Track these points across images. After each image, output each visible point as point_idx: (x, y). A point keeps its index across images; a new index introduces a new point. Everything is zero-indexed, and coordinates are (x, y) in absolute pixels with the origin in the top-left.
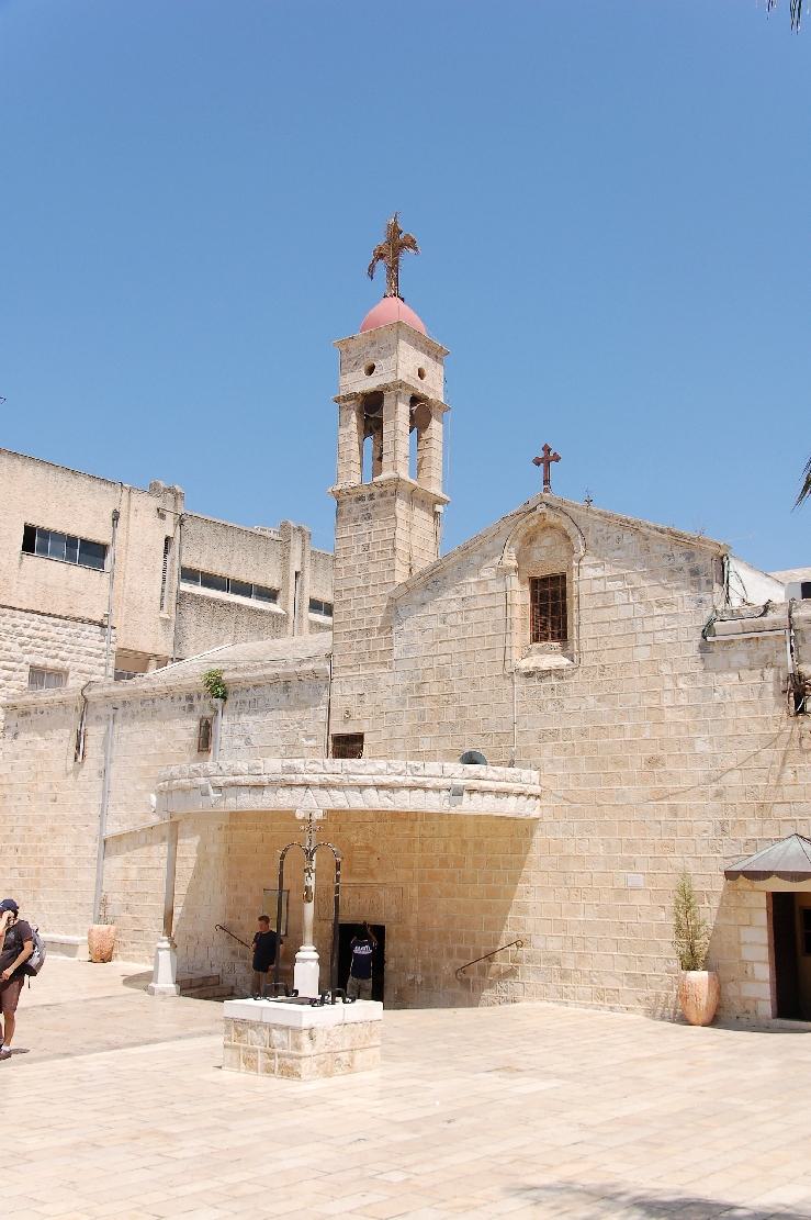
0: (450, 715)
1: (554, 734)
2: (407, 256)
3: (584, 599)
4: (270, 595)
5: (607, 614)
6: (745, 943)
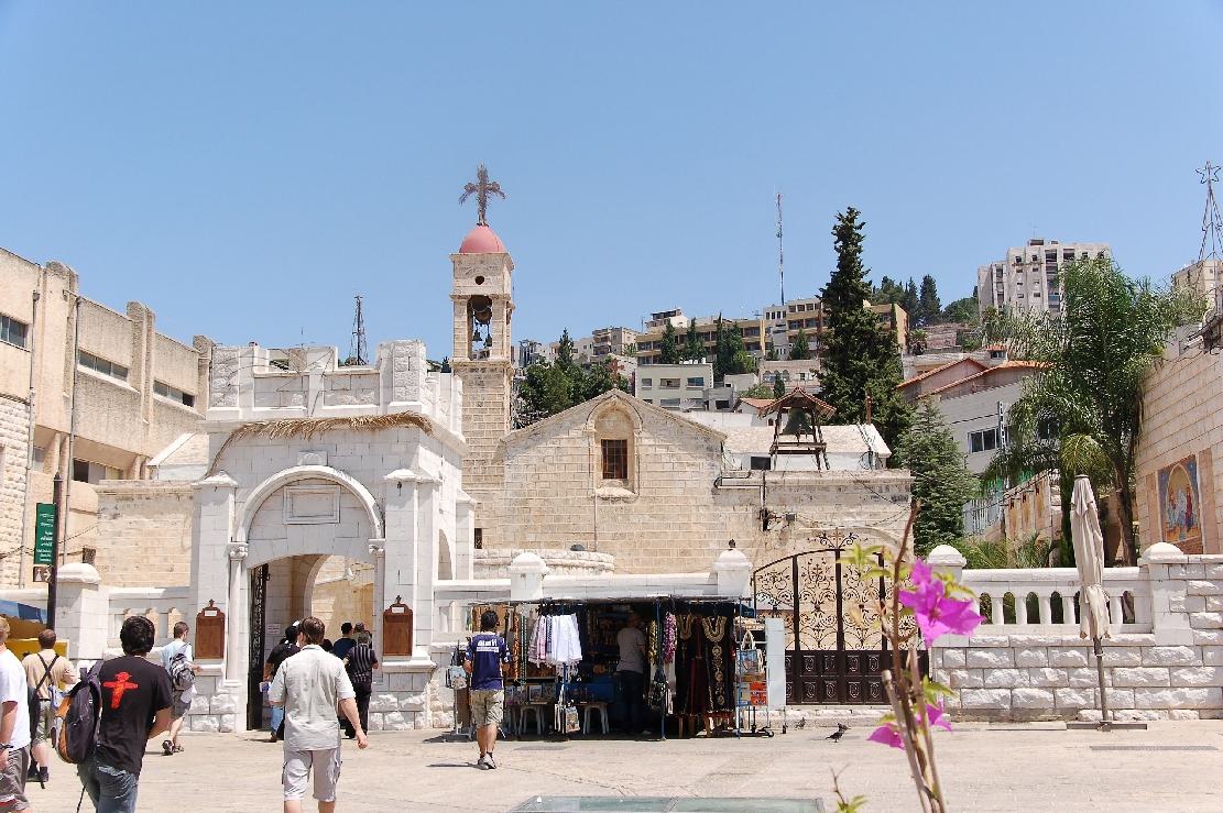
1: (623, 536)
2: (493, 200)
4: (122, 372)
5: (658, 467)
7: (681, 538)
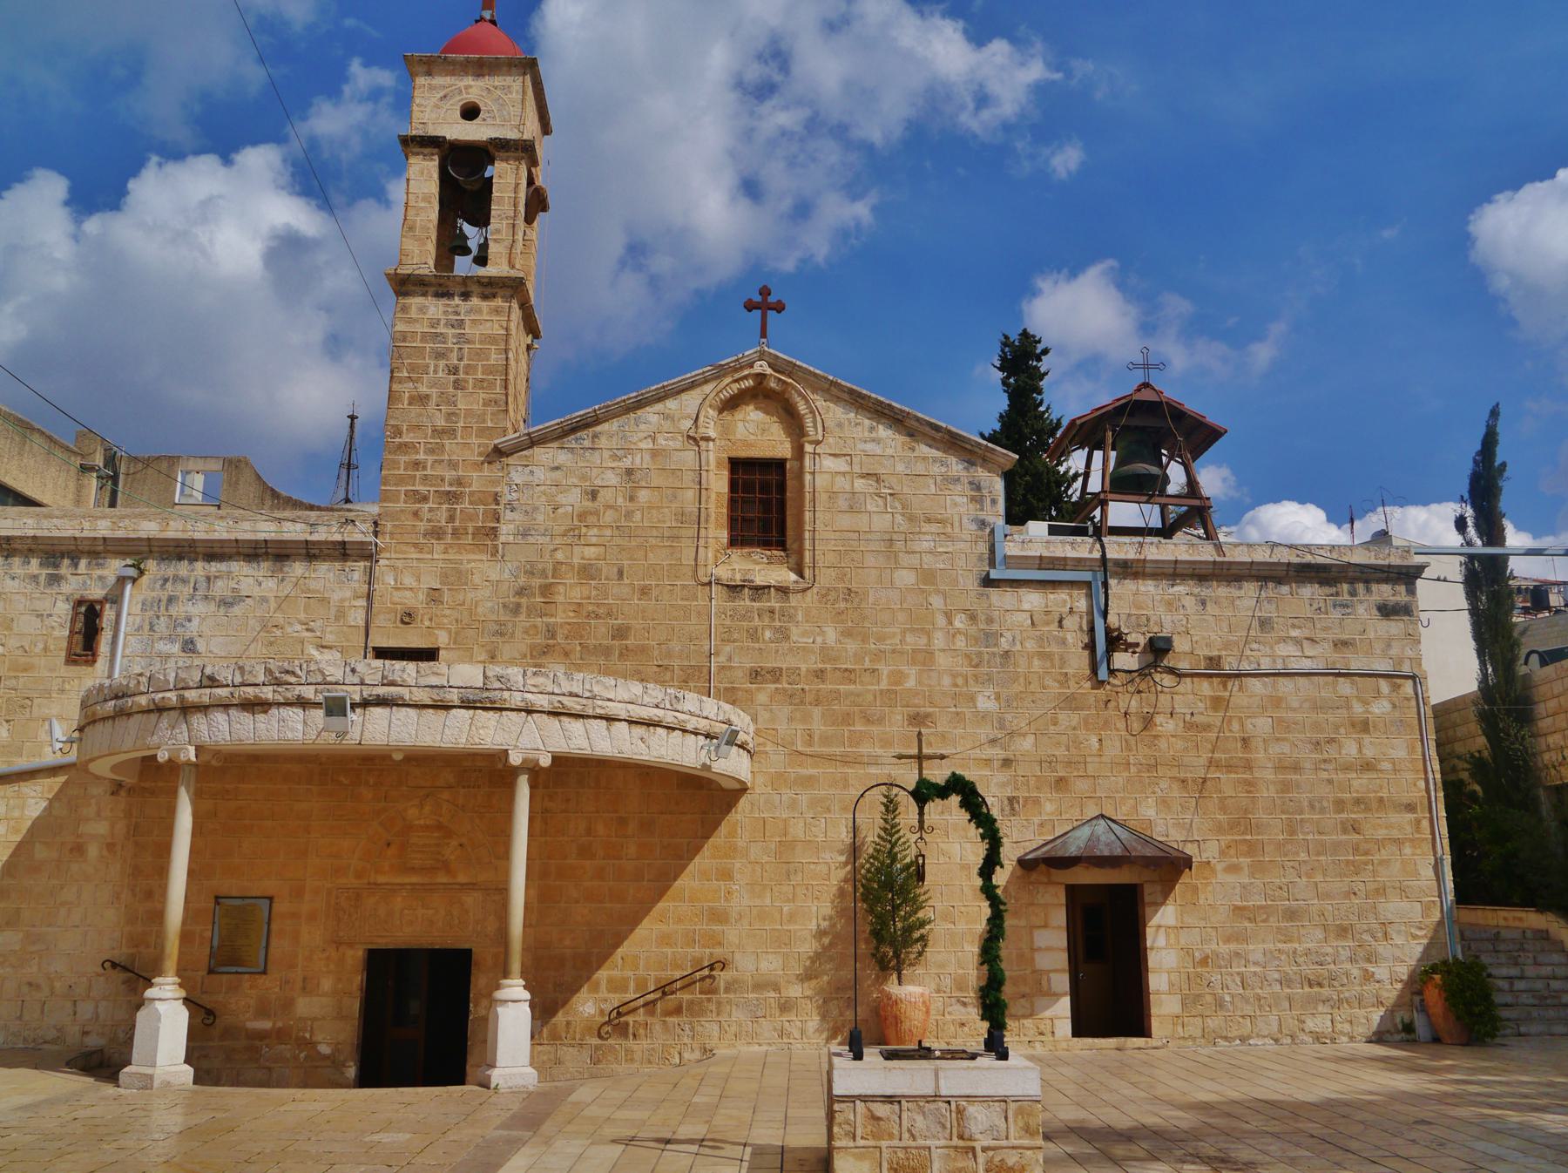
0: (600, 633)
1: (776, 674)
3: (822, 498)
6: (1039, 949)
7: (911, 683)
